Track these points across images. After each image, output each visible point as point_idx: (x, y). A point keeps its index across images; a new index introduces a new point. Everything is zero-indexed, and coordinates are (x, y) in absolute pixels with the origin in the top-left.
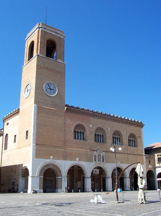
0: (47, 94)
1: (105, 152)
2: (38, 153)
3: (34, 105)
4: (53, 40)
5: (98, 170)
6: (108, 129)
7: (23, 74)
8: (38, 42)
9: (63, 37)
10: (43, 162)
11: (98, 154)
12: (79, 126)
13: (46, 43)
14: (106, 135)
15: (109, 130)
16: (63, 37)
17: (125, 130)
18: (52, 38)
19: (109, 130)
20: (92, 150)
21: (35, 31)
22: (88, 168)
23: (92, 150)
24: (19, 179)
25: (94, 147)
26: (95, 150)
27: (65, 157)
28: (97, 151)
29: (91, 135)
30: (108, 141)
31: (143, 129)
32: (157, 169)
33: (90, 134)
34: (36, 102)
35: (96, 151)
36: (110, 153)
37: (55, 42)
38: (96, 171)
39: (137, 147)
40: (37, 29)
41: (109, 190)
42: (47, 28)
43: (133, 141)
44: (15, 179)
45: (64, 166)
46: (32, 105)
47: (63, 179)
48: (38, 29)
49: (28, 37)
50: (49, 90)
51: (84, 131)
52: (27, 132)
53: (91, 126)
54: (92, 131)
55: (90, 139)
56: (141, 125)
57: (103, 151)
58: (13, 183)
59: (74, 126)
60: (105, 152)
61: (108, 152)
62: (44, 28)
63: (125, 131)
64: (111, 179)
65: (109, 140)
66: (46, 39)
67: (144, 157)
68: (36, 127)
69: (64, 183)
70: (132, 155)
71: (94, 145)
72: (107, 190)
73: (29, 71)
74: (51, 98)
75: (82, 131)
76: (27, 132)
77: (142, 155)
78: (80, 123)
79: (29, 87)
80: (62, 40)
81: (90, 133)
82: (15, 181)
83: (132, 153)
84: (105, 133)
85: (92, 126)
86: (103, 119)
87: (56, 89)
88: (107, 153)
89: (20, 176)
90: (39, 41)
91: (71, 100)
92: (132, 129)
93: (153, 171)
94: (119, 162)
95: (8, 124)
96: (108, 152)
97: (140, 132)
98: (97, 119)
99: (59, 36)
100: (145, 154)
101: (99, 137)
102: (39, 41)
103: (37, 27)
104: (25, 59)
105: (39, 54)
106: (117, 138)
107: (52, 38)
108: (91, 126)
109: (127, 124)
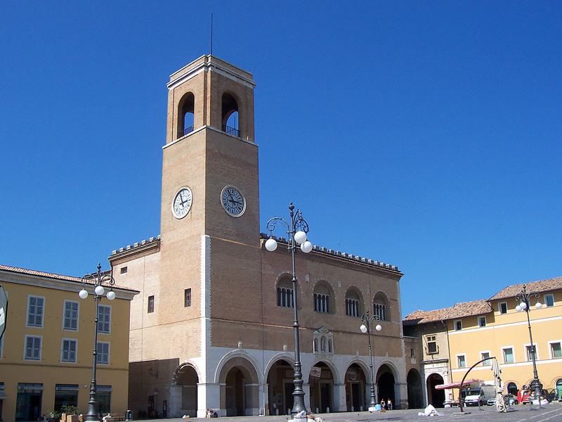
0: (227, 211)
1: (334, 331)
2: (217, 337)
3: (203, 237)
4: (234, 94)
5: (319, 369)
7: (165, 164)
9: (251, 87)
10: (225, 354)
11: (321, 335)
13: (221, 102)
16: (251, 87)
18: (231, 89)
20: (311, 329)
21: (195, 71)
22: (306, 364)
23: (311, 329)
24: (168, 390)
25: (313, 323)
27: (264, 343)
28: (320, 330)
30: (338, 309)
31: (402, 284)
32: (426, 366)
34: (208, 230)
35: (317, 330)
36: (341, 333)
37: (238, 98)
38: (315, 371)
39: (390, 321)
40: (201, 68)
41: (340, 410)
42: (221, 66)
43: (384, 307)
44: (156, 390)
45: (263, 361)
46: (199, 235)
47: (261, 388)
48: (203, 69)
49: (172, 80)
50: (231, 204)
52: (188, 291)
53: (308, 279)
56: (395, 275)
57: (330, 331)
58: (151, 399)
59: (277, 279)
60: (334, 331)
61: (338, 332)
62: (217, 68)
63: (369, 288)
64: (344, 387)
65: (340, 307)
67: (403, 341)
69: (263, 398)
70: (380, 338)
71: (314, 318)
72: (338, 409)
73: (185, 163)
74: (235, 220)
76: (188, 291)
79: (186, 195)
80: (249, 92)
81: (307, 294)
82: (157, 395)
84: (333, 291)
87: (243, 201)
89: (172, 384)
90: (209, 95)
92: (380, 284)
93: (419, 370)
94: (358, 353)
95: (124, 270)
96: (338, 332)
97: (395, 291)
99: (245, 84)
101: (322, 302)
102: (209, 95)
103: (201, 62)
104: (169, 130)
105: (208, 124)
106: (353, 304)
107: (230, 89)
108: (307, 280)
109: (371, 272)
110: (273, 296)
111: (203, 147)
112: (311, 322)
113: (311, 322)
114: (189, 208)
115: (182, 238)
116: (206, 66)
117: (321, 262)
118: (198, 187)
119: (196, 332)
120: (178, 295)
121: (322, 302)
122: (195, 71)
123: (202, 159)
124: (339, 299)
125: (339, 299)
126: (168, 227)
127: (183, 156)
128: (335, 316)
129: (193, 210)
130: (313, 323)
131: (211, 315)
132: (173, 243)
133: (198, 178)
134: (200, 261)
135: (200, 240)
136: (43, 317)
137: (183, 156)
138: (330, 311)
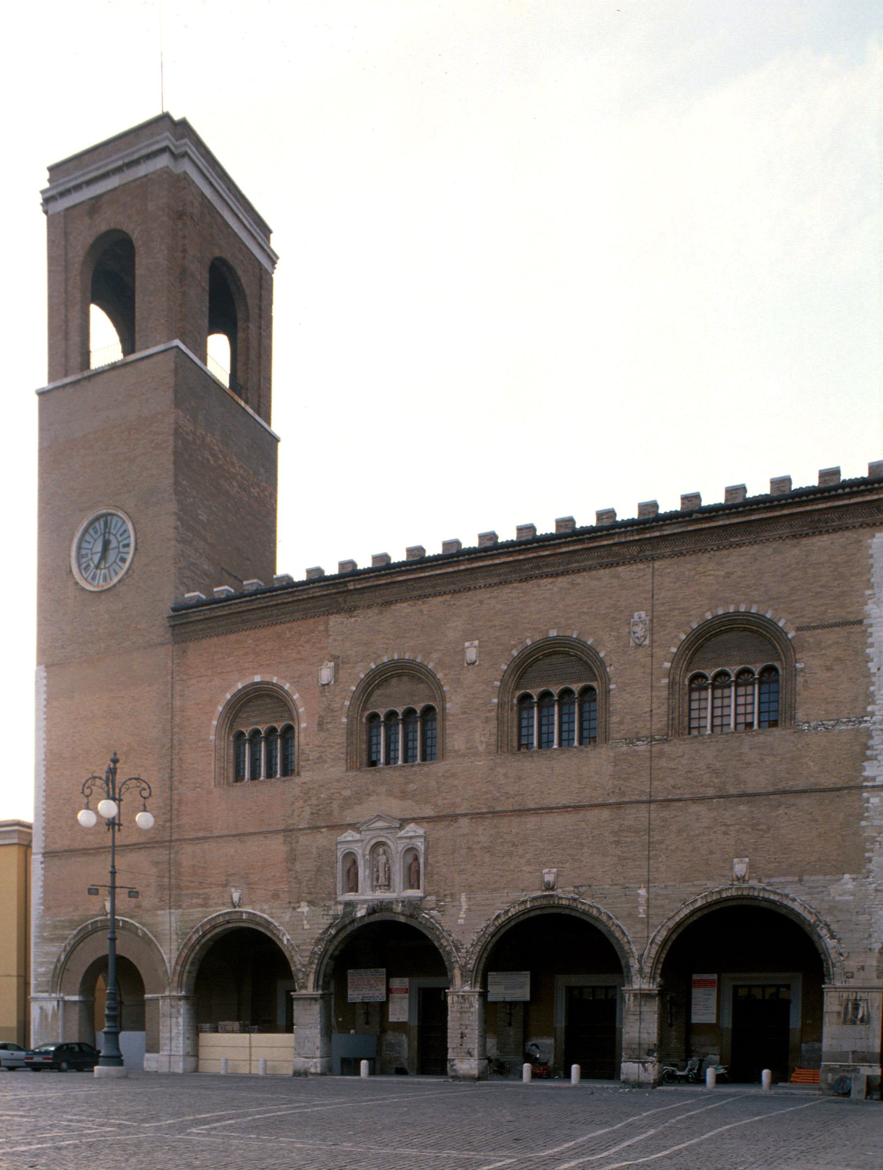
6: (463, 651)
15: (471, 654)
19: (471, 654)
25: (342, 808)
29: (323, 734)
35: (354, 826)
53: (326, 674)
54: (336, 706)
55: (320, 760)
60: (429, 819)
61: (455, 817)
78: (257, 679)
81: (320, 724)
83: (711, 792)
84: (440, 687)
88: (440, 831)
96: (455, 817)
98: (370, 612)
112: (335, 806)
113: (335, 806)
130: (342, 808)
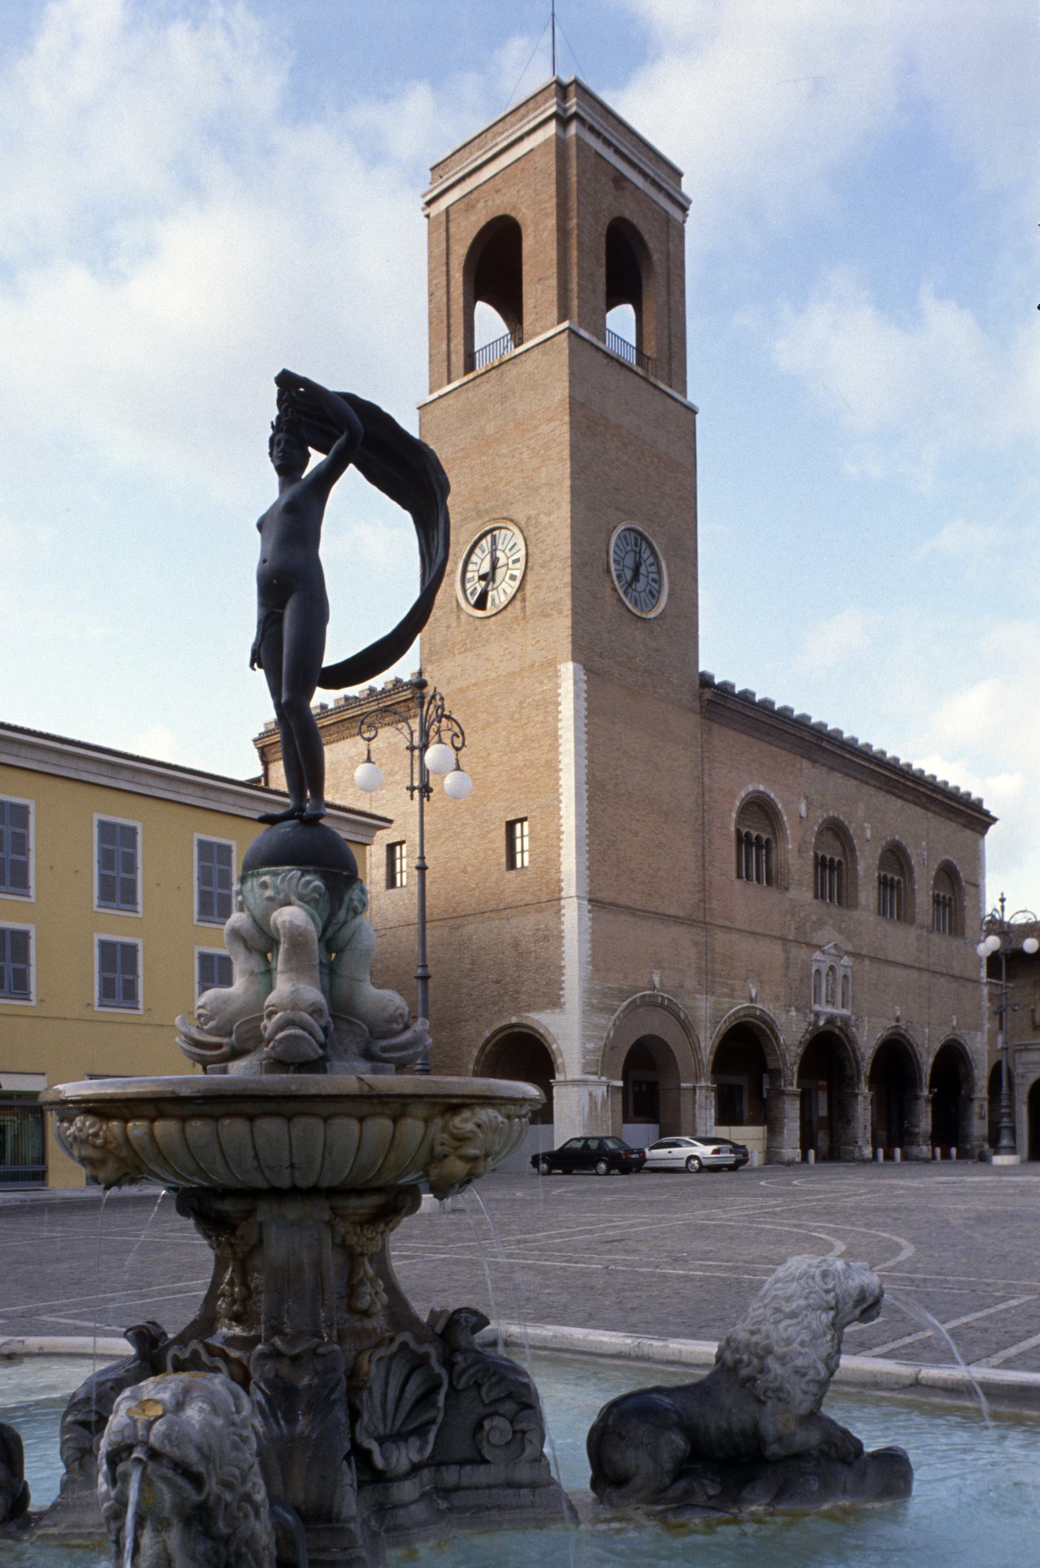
6: (864, 830)
8: (563, 232)
12: (759, 807)
14: (855, 861)
15: (868, 834)
17: (924, 844)
18: (631, 212)
20: (808, 944)
21: (520, 139)
26: (815, 941)
33: (795, 851)
34: (584, 651)
46: (551, 665)
48: (552, 128)
51: (774, 834)
56: (973, 817)
57: (847, 953)
63: (927, 841)
65: (868, 895)
66: (605, 221)
68: (589, 798)
75: (765, 836)
77: (977, 982)
78: (762, 788)
85: (808, 809)
86: (848, 775)
91: (724, 654)
97: (976, 859)
100: (989, 975)
110: (726, 851)
111: (560, 390)
114: (516, 584)
115: (494, 675)
116: (563, 120)
117: (832, 769)
118: (544, 519)
119: (546, 938)
120: (483, 837)
121: (832, 874)
122: (520, 139)
123: (559, 431)
124: (867, 866)
125: (867, 866)
126: (445, 643)
127: (490, 429)
128: (856, 914)
129: (529, 588)
131: (590, 892)
132: (461, 690)
133: (543, 492)
134: (556, 737)
135: (556, 675)
136: (196, 883)
137: (490, 429)
138: (844, 900)
